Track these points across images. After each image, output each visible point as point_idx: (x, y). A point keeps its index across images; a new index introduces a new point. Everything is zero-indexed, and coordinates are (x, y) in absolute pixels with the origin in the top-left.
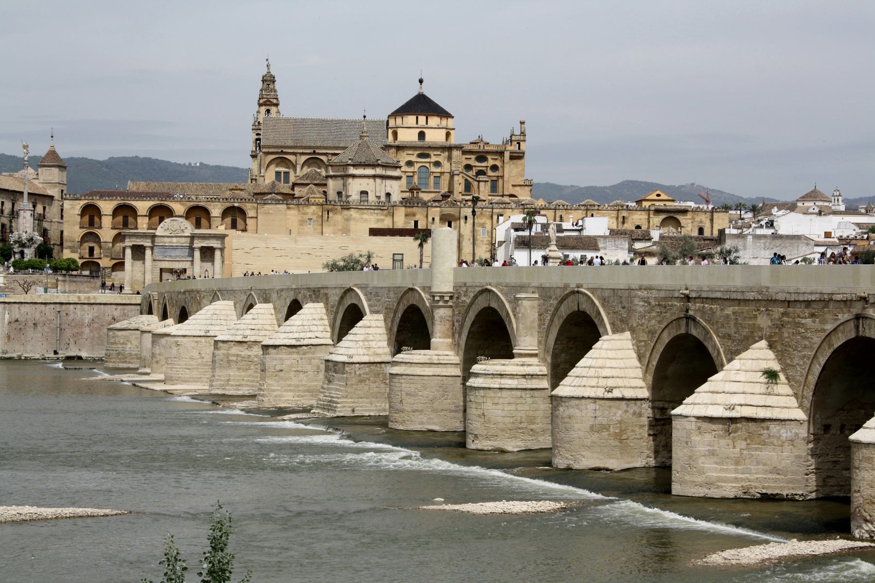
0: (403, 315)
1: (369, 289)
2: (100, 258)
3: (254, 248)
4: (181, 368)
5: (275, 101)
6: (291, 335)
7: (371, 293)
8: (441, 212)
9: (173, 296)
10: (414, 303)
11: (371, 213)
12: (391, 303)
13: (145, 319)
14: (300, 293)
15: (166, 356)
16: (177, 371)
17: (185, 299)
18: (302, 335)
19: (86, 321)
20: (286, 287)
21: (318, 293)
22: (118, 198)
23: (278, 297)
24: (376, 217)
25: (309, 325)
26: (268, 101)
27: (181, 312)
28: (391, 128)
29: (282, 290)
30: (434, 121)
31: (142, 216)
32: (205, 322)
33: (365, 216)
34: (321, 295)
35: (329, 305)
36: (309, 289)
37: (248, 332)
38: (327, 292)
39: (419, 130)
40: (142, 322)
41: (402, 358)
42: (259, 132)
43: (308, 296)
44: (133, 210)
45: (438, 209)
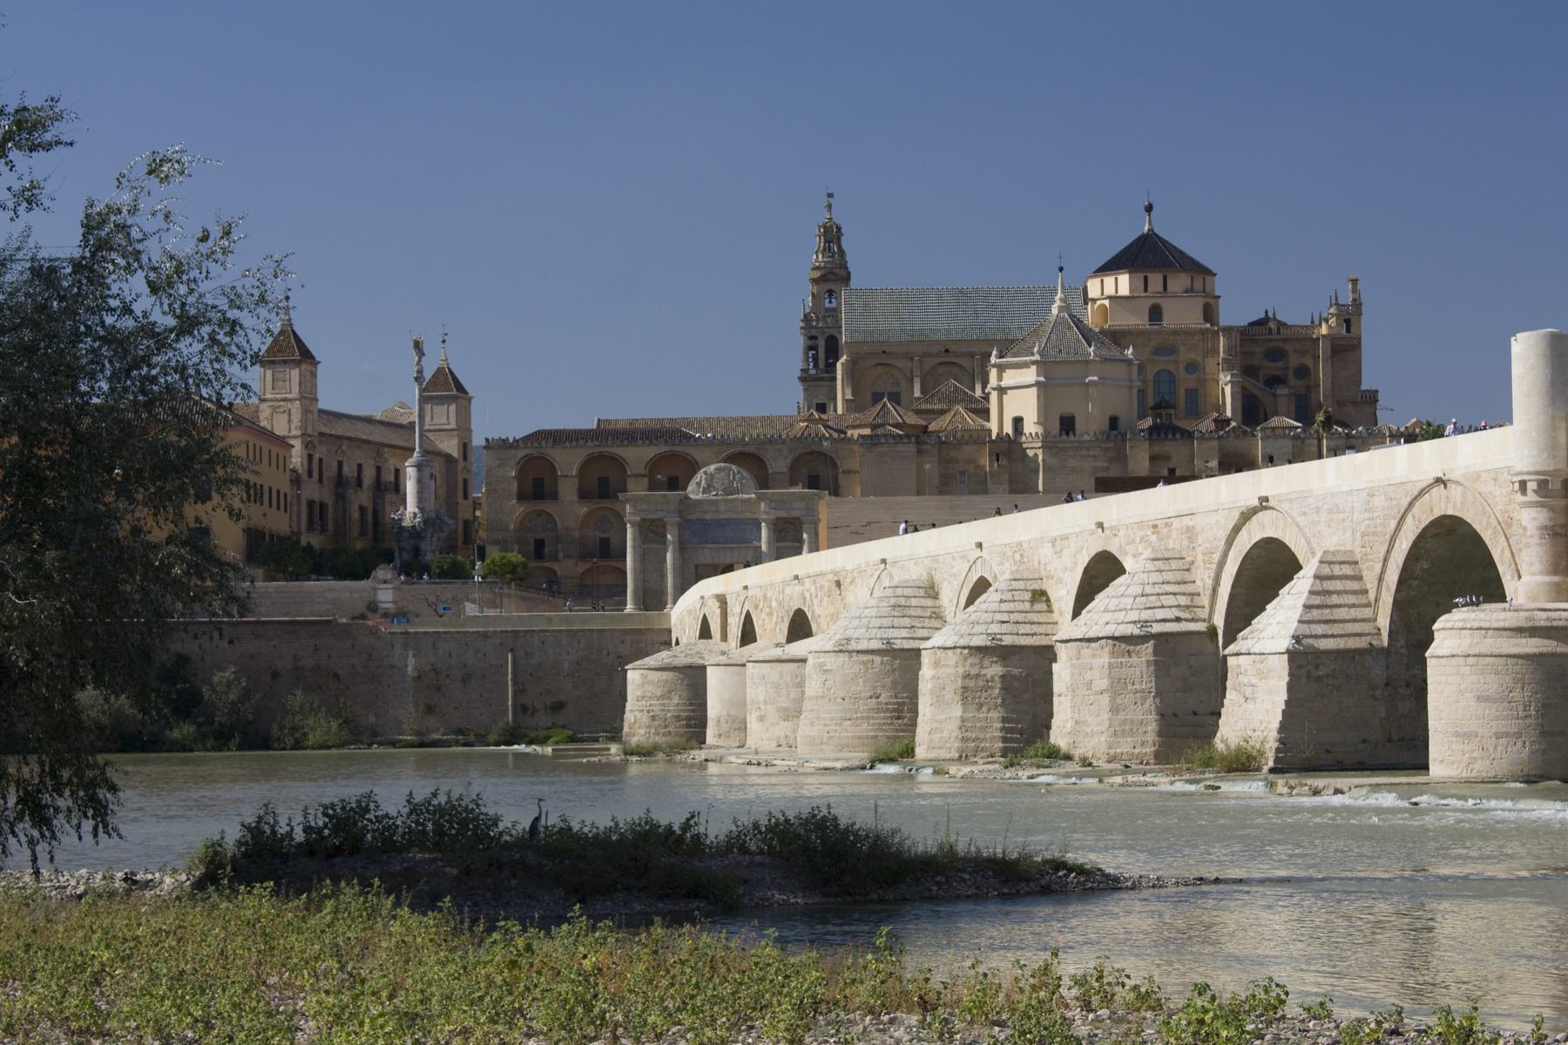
0: (1416, 545)
1: (1311, 500)
2: (556, 559)
3: (869, 524)
4: (832, 719)
5: (843, 273)
6: (1121, 616)
7: (1318, 510)
8: (1220, 449)
9: (769, 594)
10: (1450, 512)
11: (1083, 456)
12: (1378, 521)
13: (703, 647)
14: (1115, 535)
15: (779, 705)
16: (825, 725)
17: (803, 593)
18: (1146, 615)
19: (566, 665)
20: (1077, 530)
21: (1166, 530)
22: (590, 443)
23: (1056, 553)
24: (1093, 464)
25: (1158, 594)
26: (833, 275)
27: (793, 621)
28: (1094, 300)
29: (1065, 538)
30: (1179, 282)
31: (636, 476)
32: (877, 623)
33: (1072, 463)
34: (1174, 534)
35: (1199, 550)
36: (1140, 524)
37: (995, 628)
38: (1190, 523)
39: (1152, 301)
40: (698, 653)
41: (1463, 620)
42: (814, 333)
43: (1138, 540)
44: (619, 464)
45: (1215, 443)
